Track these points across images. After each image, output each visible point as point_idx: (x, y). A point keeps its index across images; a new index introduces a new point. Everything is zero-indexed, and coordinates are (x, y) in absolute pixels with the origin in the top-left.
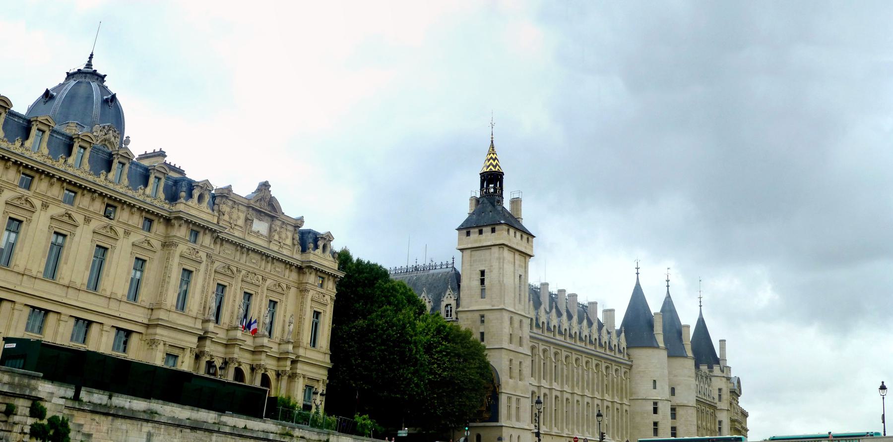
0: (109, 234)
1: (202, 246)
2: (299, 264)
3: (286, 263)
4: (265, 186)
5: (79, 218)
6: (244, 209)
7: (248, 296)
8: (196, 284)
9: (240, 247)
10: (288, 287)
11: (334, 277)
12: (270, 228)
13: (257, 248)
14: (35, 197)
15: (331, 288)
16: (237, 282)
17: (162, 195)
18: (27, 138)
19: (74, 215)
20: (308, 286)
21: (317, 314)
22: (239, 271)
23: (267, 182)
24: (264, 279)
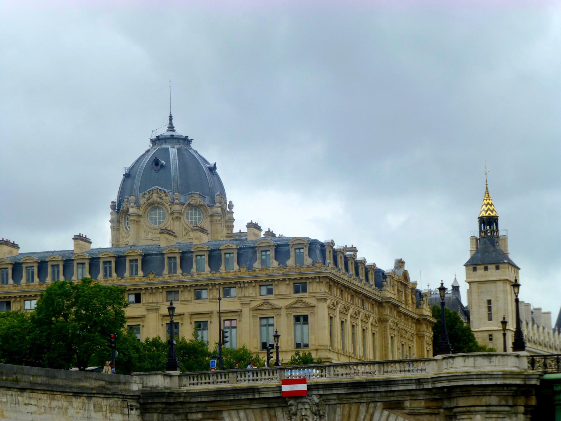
3: (412, 318)
23: (401, 260)
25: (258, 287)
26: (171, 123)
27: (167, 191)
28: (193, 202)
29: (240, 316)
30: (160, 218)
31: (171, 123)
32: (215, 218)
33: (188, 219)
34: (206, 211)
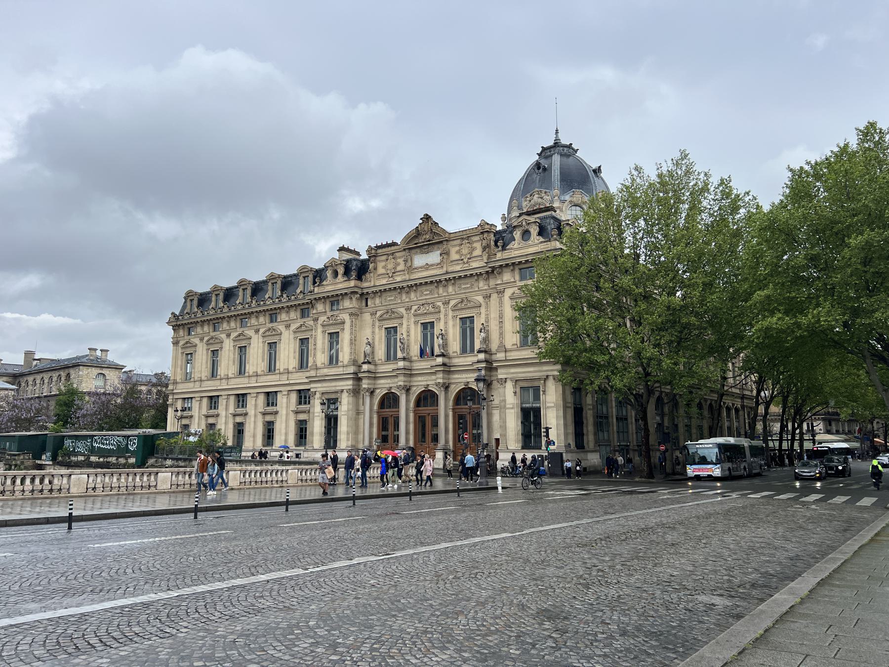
10: (488, 297)
22: (409, 309)
24: (446, 303)
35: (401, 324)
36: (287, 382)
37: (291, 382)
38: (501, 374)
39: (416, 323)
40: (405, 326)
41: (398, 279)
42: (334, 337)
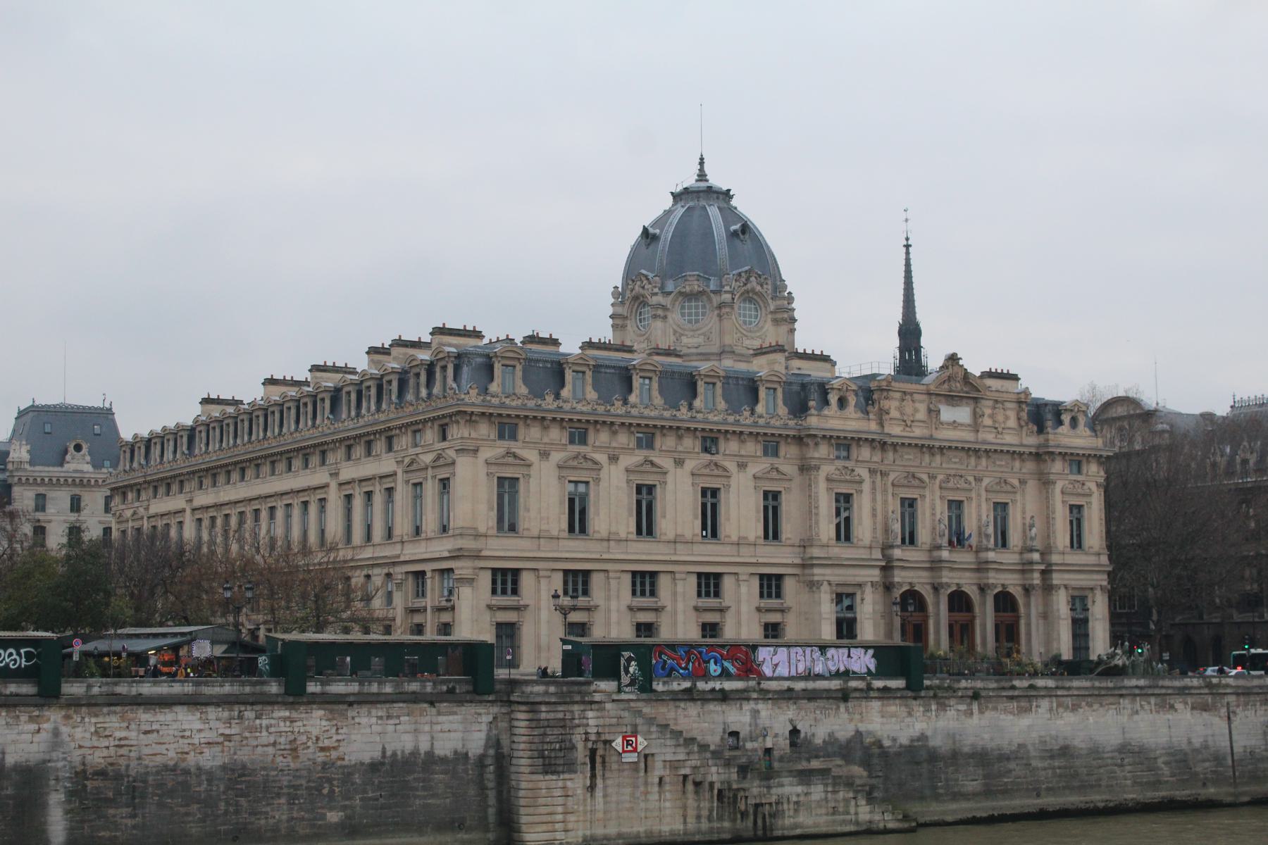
0: (716, 472)
1: (857, 461)
2: (1033, 450)
4: (953, 359)
5: (666, 463)
6: (925, 397)
7: (956, 506)
8: (860, 508)
9: (927, 448)
11: (1098, 458)
12: (975, 413)
13: (954, 445)
14: (594, 452)
15: (1094, 472)
16: (933, 492)
17: (782, 410)
18: (562, 385)
19: (655, 460)
20: (1052, 477)
21: (1076, 510)
24: (978, 480)
25: (410, 434)
26: (702, 169)
27: (651, 275)
28: (688, 289)
29: (395, 481)
30: (697, 314)
31: (702, 169)
32: (724, 310)
33: (683, 315)
34: (710, 300)
35: (923, 497)
36: (754, 560)
37: (761, 560)
38: (1057, 579)
39: (942, 498)
40: (927, 500)
41: (918, 432)
42: (844, 501)
